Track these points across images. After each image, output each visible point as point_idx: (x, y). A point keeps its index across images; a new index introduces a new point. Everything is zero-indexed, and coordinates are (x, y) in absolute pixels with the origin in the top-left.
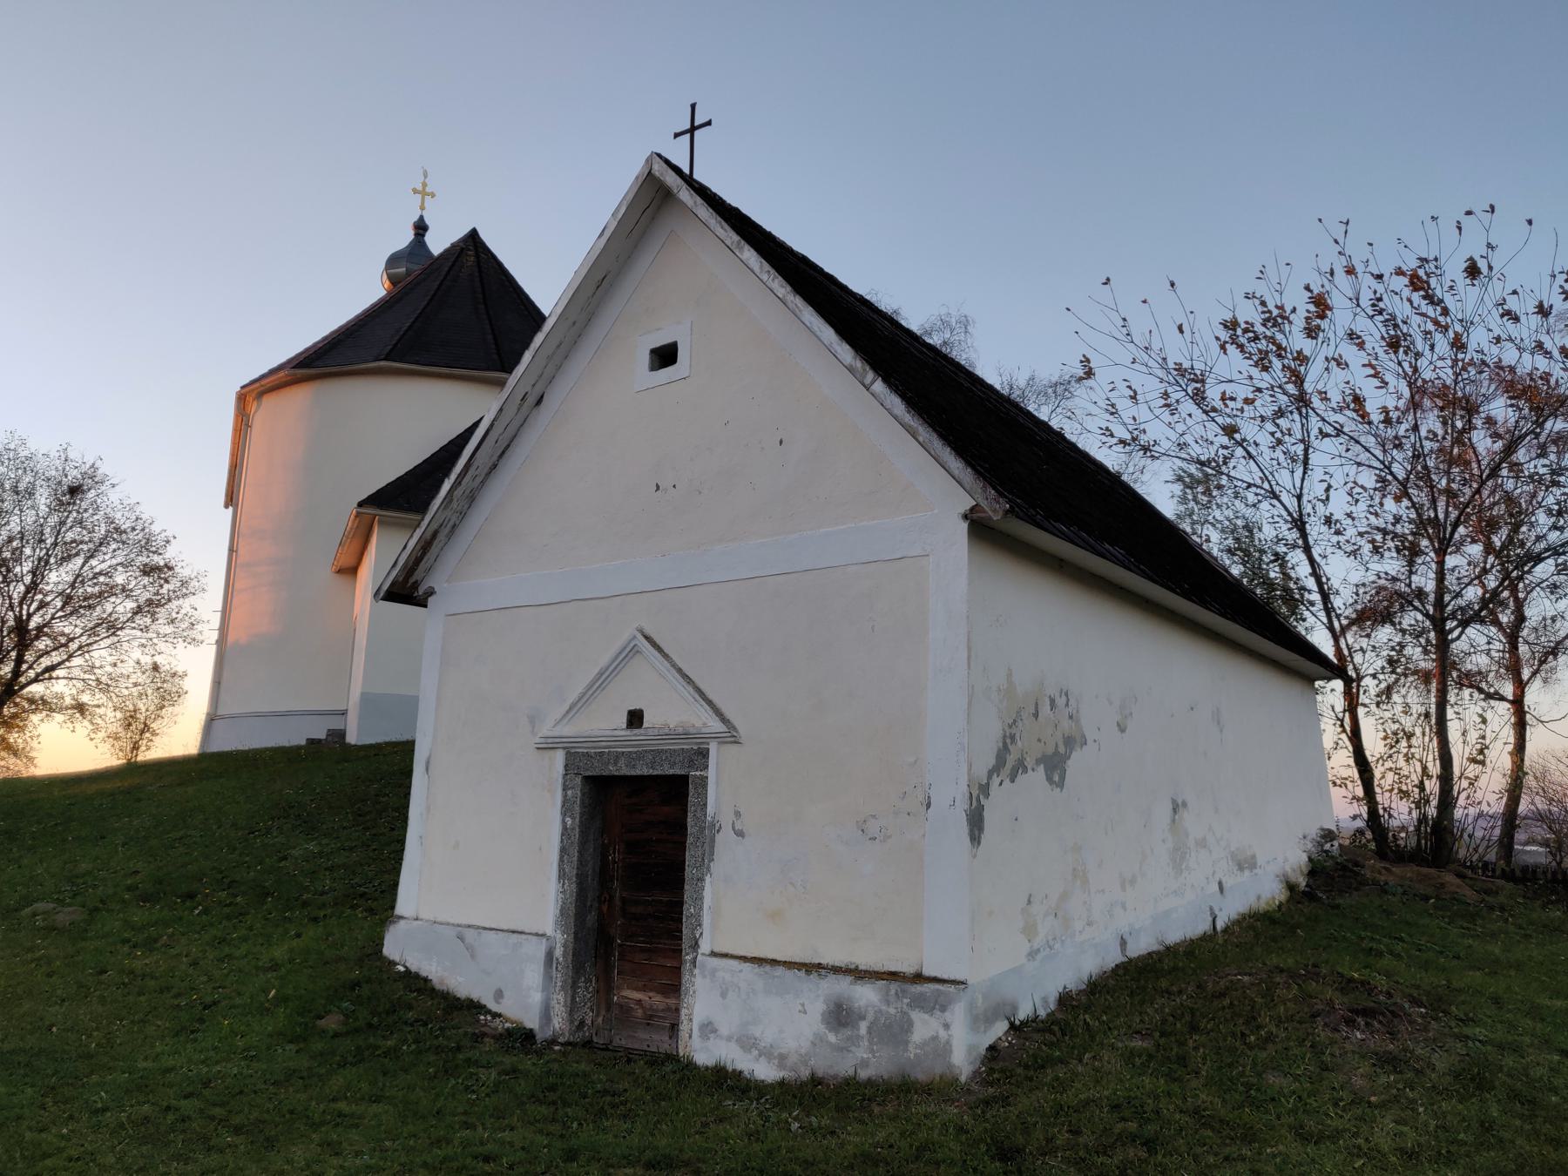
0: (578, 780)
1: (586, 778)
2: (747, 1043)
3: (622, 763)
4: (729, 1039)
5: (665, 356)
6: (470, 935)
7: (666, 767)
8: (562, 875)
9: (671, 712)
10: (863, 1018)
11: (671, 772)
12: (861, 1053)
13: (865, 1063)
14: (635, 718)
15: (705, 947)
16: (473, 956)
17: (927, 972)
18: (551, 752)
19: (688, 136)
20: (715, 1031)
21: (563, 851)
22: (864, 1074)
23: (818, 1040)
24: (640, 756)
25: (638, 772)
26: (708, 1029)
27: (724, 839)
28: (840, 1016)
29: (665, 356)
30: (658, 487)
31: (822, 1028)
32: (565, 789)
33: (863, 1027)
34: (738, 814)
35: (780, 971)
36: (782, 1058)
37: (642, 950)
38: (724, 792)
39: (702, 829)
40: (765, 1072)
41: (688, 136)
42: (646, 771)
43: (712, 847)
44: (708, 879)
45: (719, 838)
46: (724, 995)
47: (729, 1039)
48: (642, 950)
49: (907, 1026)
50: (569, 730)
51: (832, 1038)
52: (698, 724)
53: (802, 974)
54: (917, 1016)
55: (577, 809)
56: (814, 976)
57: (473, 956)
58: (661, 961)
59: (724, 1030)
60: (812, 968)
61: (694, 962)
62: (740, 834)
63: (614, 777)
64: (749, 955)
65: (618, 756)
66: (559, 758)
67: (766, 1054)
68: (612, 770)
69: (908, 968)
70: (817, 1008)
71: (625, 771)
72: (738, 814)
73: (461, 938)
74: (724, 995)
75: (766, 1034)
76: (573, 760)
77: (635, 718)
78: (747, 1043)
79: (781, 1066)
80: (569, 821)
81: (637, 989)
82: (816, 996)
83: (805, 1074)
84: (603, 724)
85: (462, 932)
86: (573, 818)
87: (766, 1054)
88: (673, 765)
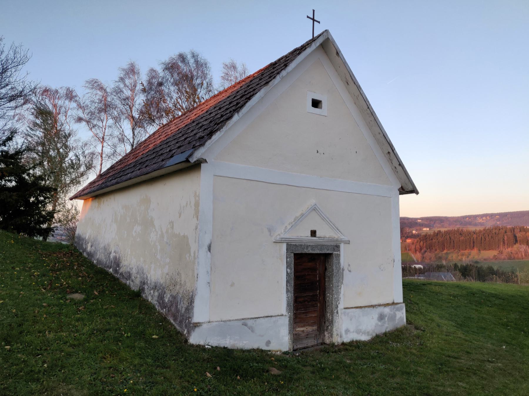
0: (293, 255)
1: (295, 254)
2: (358, 332)
3: (309, 249)
4: (353, 332)
5: (316, 104)
6: (250, 323)
7: (326, 250)
8: (288, 291)
9: (325, 233)
10: (386, 316)
11: (328, 252)
12: (386, 325)
13: (387, 328)
14: (313, 233)
15: (341, 306)
16: (253, 331)
17: (395, 302)
18: (280, 244)
19: (315, 22)
20: (349, 331)
21: (287, 282)
22: (387, 330)
23: (377, 325)
24: (317, 246)
25: (316, 252)
26: (347, 331)
27: (346, 272)
28: (381, 317)
29: (316, 104)
30: (318, 152)
31: (377, 322)
32: (287, 258)
33: (386, 319)
34: (349, 265)
35: (367, 309)
36: (368, 332)
37: (304, 313)
38: (345, 258)
39: (338, 271)
40: (364, 338)
41: (315, 22)
42: (318, 252)
43: (343, 276)
44: (342, 286)
45: (344, 272)
46: (351, 320)
47: (353, 332)
48: (304, 313)
49: (395, 315)
50: (287, 236)
51: (380, 323)
52: (336, 237)
53: (372, 308)
54: (397, 313)
55: (293, 266)
56: (375, 308)
57: (253, 331)
58: (310, 315)
59: (352, 330)
60: (373, 306)
61: (337, 313)
62: (350, 271)
63: (306, 254)
64: (354, 306)
65: (308, 246)
66: (284, 246)
67: (364, 333)
68: (306, 251)
69: (390, 302)
70: (376, 316)
71: (311, 252)
72: (349, 265)
73: (245, 325)
74: (351, 320)
75: (363, 328)
76: (290, 247)
77: (313, 233)
78: (358, 332)
79: (368, 335)
80: (289, 270)
81: (302, 327)
82: (375, 313)
83: (374, 335)
84: (302, 234)
85: (244, 322)
86: (291, 269)
87: (364, 333)
88: (328, 250)
